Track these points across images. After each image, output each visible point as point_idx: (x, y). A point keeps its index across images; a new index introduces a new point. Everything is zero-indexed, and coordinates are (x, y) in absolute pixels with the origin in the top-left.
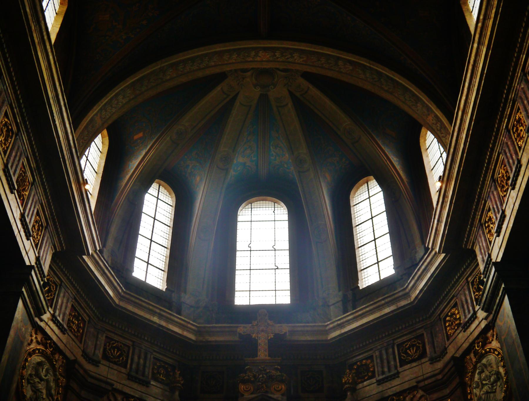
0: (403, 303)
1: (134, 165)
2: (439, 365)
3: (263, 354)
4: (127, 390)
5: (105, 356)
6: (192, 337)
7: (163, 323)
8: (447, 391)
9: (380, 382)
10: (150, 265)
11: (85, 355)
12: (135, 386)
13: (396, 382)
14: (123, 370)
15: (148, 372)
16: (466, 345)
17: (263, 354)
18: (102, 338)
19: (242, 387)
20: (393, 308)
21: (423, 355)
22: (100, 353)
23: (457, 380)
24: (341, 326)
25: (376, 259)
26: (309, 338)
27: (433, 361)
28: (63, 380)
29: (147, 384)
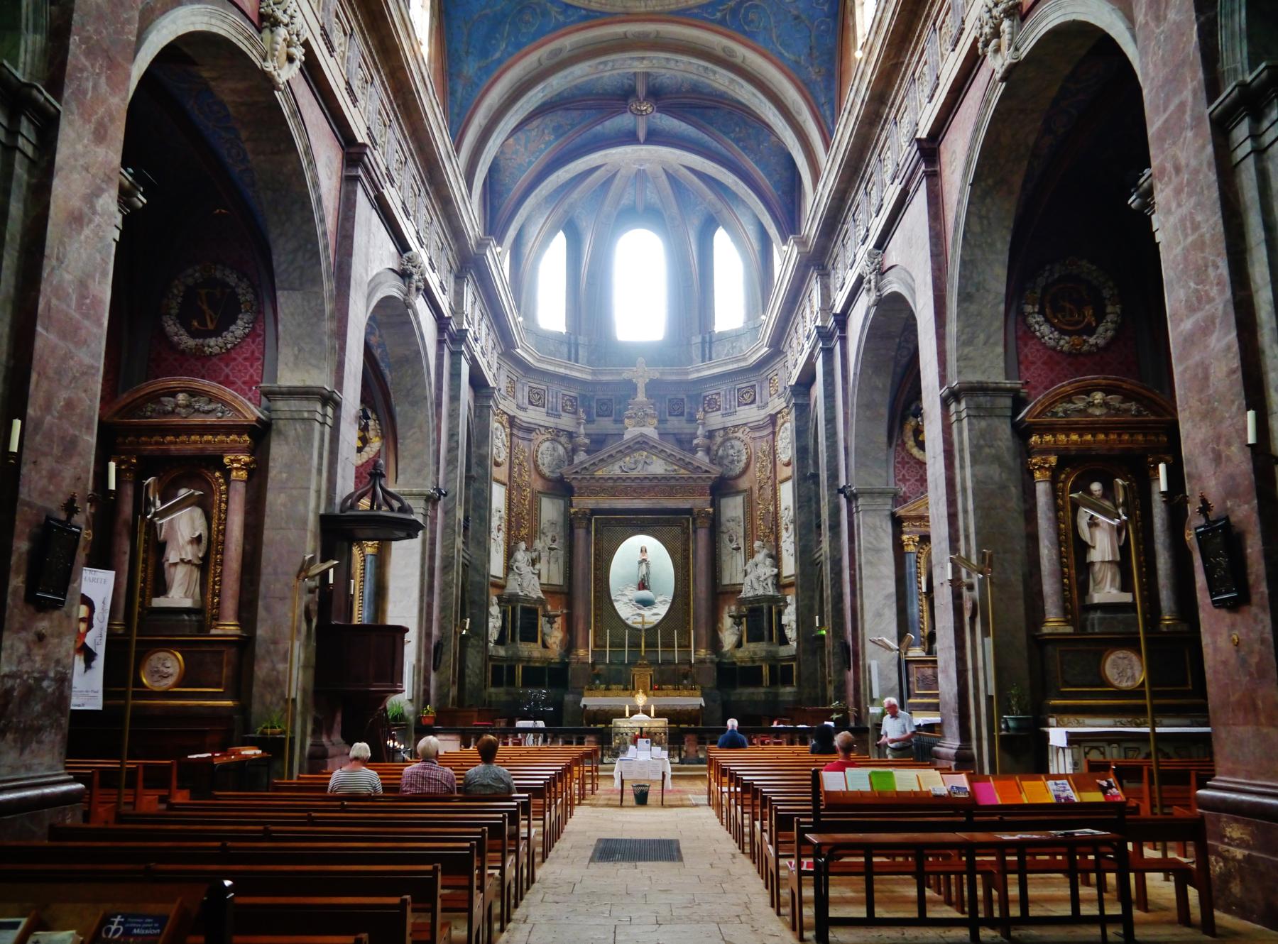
0: (743, 364)
1: (533, 232)
2: (763, 414)
3: (641, 397)
4: (547, 424)
5: (531, 403)
6: (589, 377)
7: (568, 372)
8: (765, 432)
9: (723, 415)
10: (551, 311)
11: (519, 407)
12: (552, 419)
13: (732, 418)
14: (544, 410)
15: (560, 408)
16: (778, 409)
17: (641, 397)
18: (527, 389)
19: (626, 421)
20: (735, 366)
21: (753, 402)
22: (526, 401)
23: (770, 430)
24: (698, 371)
25: (730, 308)
26: (674, 378)
27: (759, 408)
28: (508, 430)
29: (559, 416)
